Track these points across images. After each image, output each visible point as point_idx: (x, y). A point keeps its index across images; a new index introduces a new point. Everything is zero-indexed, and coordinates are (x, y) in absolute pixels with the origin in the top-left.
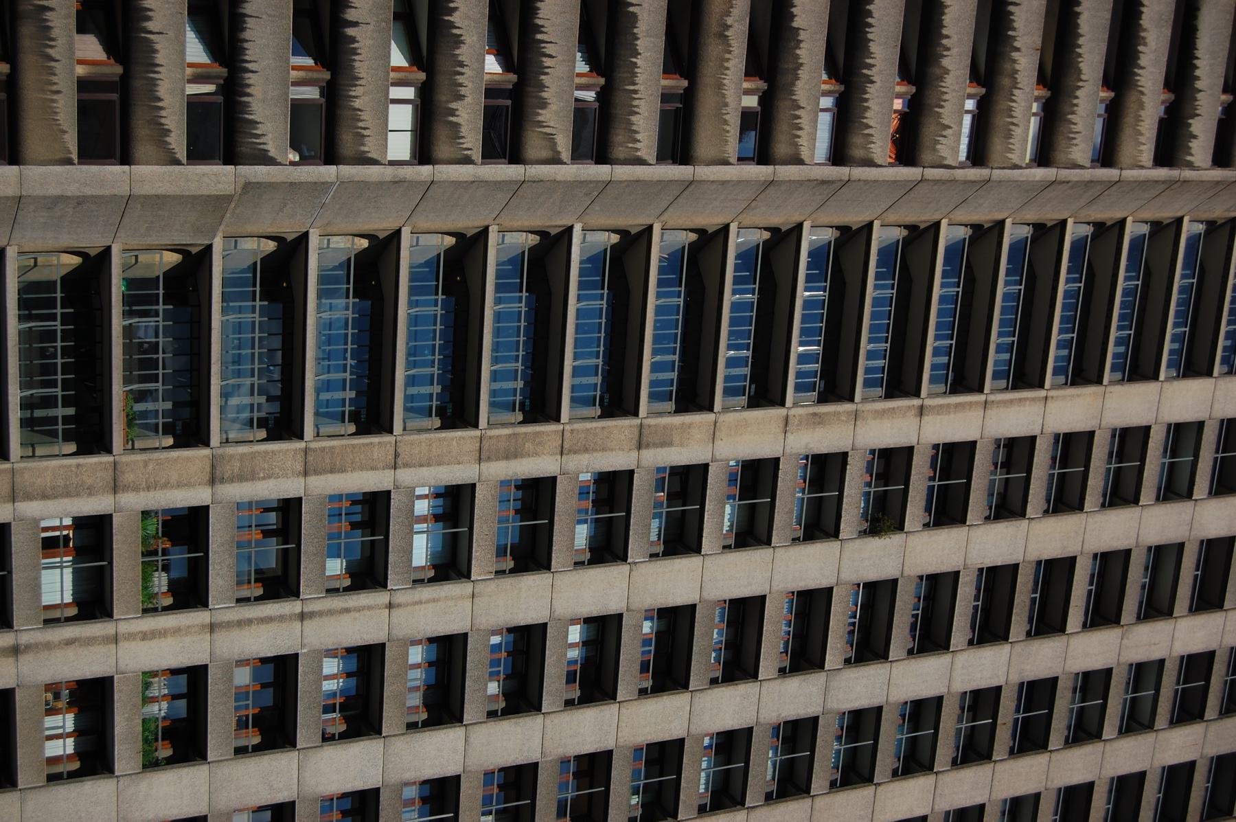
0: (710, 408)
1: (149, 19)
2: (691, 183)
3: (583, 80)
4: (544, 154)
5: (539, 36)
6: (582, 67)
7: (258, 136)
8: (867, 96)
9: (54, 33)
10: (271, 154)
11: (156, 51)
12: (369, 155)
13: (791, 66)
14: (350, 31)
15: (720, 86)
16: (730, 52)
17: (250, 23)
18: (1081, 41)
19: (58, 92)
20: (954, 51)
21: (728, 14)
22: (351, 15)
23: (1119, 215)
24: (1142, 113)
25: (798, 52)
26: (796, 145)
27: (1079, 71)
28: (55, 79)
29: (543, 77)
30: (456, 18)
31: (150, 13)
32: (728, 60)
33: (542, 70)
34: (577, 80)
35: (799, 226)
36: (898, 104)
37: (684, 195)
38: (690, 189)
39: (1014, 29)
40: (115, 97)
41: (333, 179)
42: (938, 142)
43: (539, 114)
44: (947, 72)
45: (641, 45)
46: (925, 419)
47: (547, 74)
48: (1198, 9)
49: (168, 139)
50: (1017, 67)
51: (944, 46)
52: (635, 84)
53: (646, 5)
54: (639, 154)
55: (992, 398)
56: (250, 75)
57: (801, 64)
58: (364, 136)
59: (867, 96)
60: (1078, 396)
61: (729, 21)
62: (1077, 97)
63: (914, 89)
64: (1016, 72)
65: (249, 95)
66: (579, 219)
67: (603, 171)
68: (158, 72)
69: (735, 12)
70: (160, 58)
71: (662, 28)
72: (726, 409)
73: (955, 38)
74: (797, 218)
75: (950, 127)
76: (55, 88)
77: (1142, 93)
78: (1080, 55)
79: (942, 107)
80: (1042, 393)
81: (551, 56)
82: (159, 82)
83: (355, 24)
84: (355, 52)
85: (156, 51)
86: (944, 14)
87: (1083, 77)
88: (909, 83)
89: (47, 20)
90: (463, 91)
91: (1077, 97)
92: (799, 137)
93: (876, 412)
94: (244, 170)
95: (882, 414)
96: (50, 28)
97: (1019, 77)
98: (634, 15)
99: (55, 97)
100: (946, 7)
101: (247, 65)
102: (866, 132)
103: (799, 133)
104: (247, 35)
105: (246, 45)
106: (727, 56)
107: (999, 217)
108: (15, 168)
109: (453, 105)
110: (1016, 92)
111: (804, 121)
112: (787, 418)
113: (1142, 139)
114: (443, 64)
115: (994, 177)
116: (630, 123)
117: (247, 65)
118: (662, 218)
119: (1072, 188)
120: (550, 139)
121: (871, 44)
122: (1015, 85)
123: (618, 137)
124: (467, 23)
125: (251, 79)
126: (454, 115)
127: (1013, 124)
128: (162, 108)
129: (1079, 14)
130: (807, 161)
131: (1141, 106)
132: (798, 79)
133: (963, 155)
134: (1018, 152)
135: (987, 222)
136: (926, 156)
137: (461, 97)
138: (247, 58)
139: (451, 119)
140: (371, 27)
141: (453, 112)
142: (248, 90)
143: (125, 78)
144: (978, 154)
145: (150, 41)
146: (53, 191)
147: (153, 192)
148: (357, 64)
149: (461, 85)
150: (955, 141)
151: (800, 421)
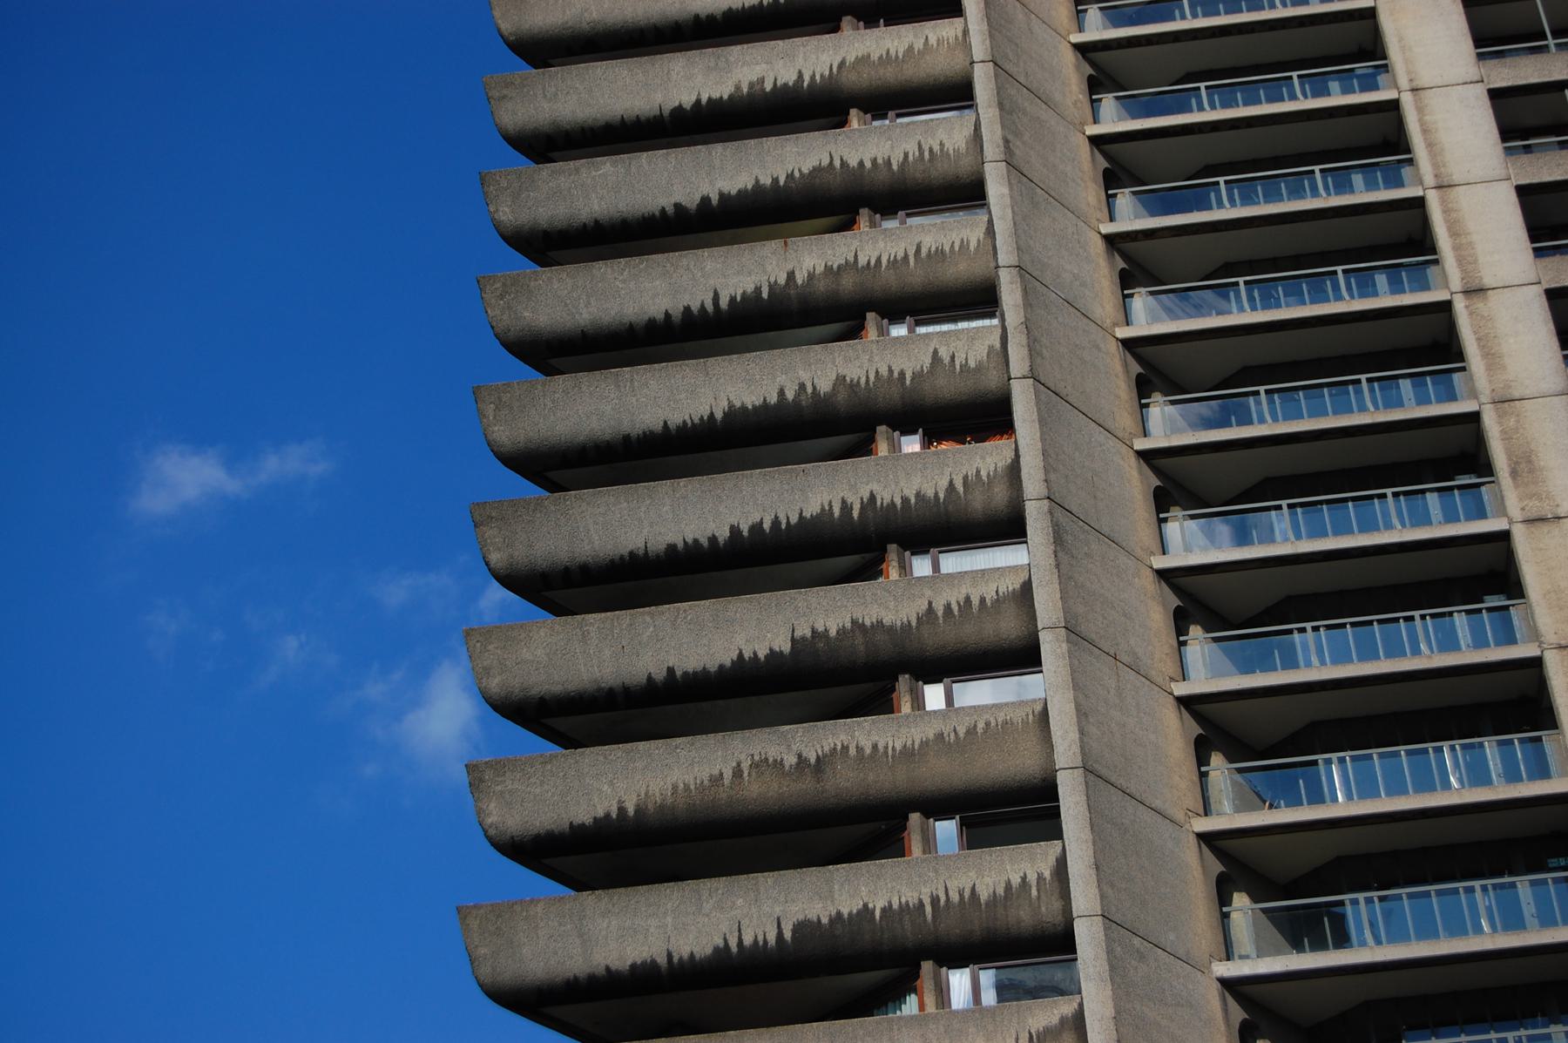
0: (1537, 663)
2: (1088, 770)
3: (930, 1000)
6: (911, 1005)
8: (898, 502)
13: (859, 640)
15: (908, 754)
16: (845, 748)
18: (766, 181)
20: (805, 376)
21: (778, 764)
23: (1069, 57)
24: (875, 57)
25: (833, 633)
26: (998, 601)
27: (817, 170)
32: (859, 749)
34: (931, 1008)
35: (1164, 575)
36: (912, 445)
37: (1121, 782)
38: (1104, 772)
39: (758, 290)
42: (964, 366)
44: (841, 379)
45: (848, 906)
46: (1488, 281)
48: (697, 17)
50: (820, 269)
51: (797, 395)
52: (921, 904)
53: (778, 910)
54: (1047, 874)
55: (1429, 180)
57: (854, 622)
59: (898, 502)
60: (1401, 40)
61: (790, 760)
62: (861, 163)
63: (882, 429)
64: (828, 269)
66: (1203, 969)
67: (1087, 935)
69: (773, 753)
71: (813, 874)
72: (1535, 635)
73: (781, 379)
74: (1149, 582)
75: (936, 352)
77: (842, 64)
78: (790, 176)
79: (902, 374)
80: (1407, 101)
86: (744, 408)
87: (826, 162)
88: (872, 440)
91: (861, 163)
92: (982, 600)
93: (1490, 368)
95: (1493, 359)
97: (836, 262)
98: (799, 928)
100: (731, 406)
102: (960, 488)
103: (975, 601)
106: (852, 751)
107: (1098, 246)
110: (862, 261)
111: (954, 596)
112: (1529, 521)
113: (919, 45)
115: (1013, 260)
116: (994, 900)
118: (1179, 816)
119: (1018, 134)
121: (807, 514)
122: (851, 266)
123: (1023, 917)
127: (918, 251)
129: (721, 195)
130: (1024, 577)
131: (864, 60)
132: (880, 623)
133: (995, 322)
134: (965, 233)
135: (1112, 263)
136: (992, 381)
144: (978, 299)
150: (963, 343)
151: (1531, 496)
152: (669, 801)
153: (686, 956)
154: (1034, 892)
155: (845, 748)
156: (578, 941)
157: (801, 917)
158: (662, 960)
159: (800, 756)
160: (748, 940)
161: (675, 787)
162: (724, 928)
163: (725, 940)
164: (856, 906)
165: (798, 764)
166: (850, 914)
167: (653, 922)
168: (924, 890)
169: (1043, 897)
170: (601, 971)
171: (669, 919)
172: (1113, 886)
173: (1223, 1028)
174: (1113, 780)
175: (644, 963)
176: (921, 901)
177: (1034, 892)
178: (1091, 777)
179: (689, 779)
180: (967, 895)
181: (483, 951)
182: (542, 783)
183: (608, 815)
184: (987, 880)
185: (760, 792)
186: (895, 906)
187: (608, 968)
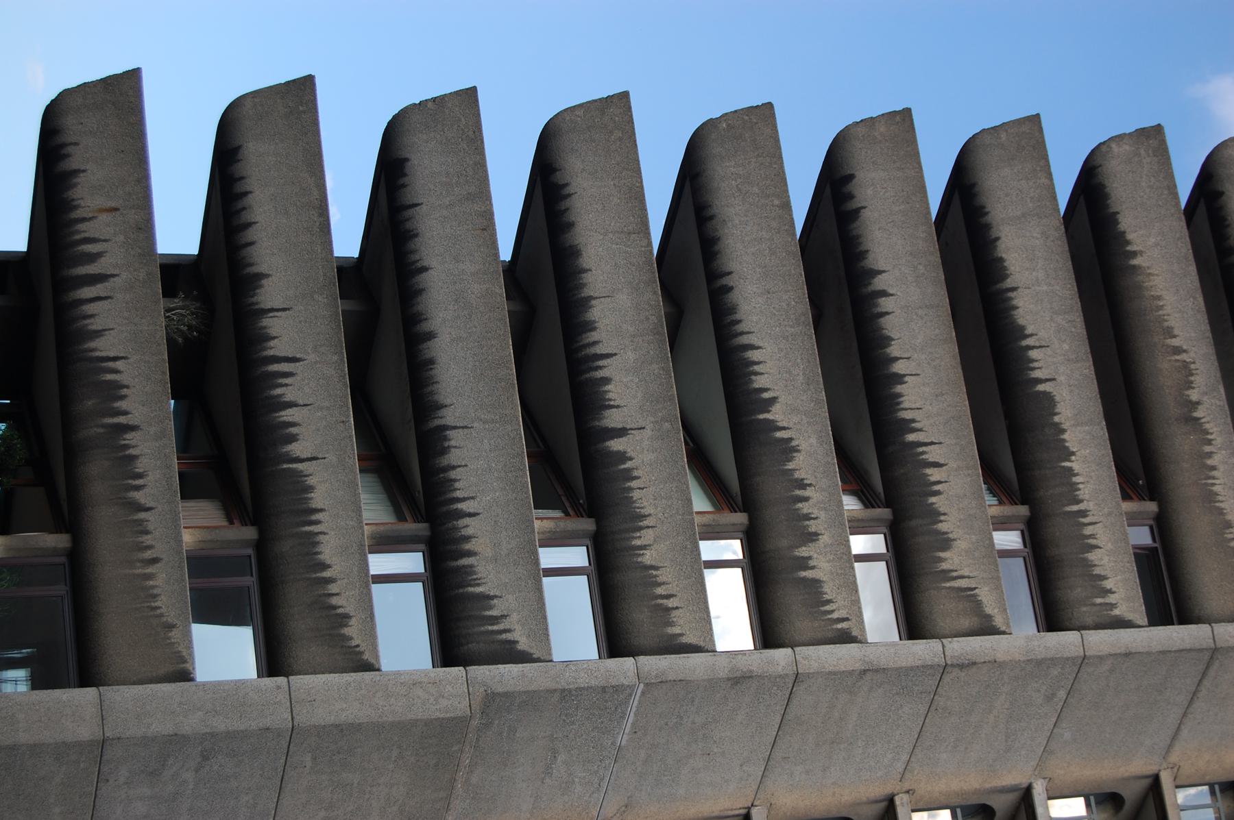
1: (293, 439)
4: (966, 623)
5: (911, 437)
7: (495, 620)
9: (140, 467)
10: (521, 647)
11: (310, 489)
12: (684, 640)
14: (616, 445)
15: (1210, 497)
16: (1209, 442)
17: (455, 438)
19: (155, 561)
21: (1189, 385)
22: (612, 419)
28: (147, 540)
29: (933, 500)
30: (776, 414)
31: (293, 430)
32: (1210, 455)
33: (929, 490)
37: (1203, 693)
38: (1212, 673)
40: (250, 581)
41: (631, 679)
43: (941, 560)
45: (1071, 438)
47: (937, 493)
49: (346, 631)
52: (1079, 502)
53: (1062, 378)
54: (1116, 612)
56: (466, 521)
58: (668, 610)
61: (1194, 395)
65: (470, 554)
68: (318, 522)
69: (1199, 380)
70: (318, 498)
76: (148, 554)
81: (937, 465)
82: (321, 538)
83: (622, 432)
84: (628, 476)
85: (310, 489)
89: (127, 447)
90: (813, 526)
94: (480, 672)
96: (133, 458)
98: (1048, 398)
99: (149, 570)
101: (460, 506)
104: (453, 457)
105: (453, 474)
106: (1207, 449)
108: (90, 693)
109: (803, 552)
114: (769, 488)
116: (1090, 565)
117: (460, 506)
118: (1173, 758)
120: (969, 597)
123: (1073, 591)
124: (795, 419)
125: (470, 527)
126: (807, 568)
128: (331, 580)
137: (813, 537)
138: (458, 494)
139: (803, 574)
140: (648, 433)
141: (804, 563)
142: (467, 546)
143: (261, 546)
145: (300, 474)
146: (160, 726)
147: (331, 719)
148: (636, 495)
149: (808, 517)
152: (1147, 293)
153: (1015, 302)
154: (1099, 601)
155: (1209, 442)
156: (1019, 213)
157: (1057, 398)
158: (1009, 283)
159: (1198, 403)
160: (1033, 354)
161: (1159, 298)
162: (1042, 334)
163: (1031, 335)
164: (1072, 445)
165: (1191, 402)
166: (1064, 440)
167: (1041, 275)
168: (1091, 504)
169: (1097, 608)
170: (994, 233)
171: (1045, 288)
172: (1111, 671)
173: (987, 786)
174: (1206, 683)
175: (1005, 269)
176: (1082, 501)
177: (1099, 601)
178: (1207, 656)
179: (1168, 310)
180: (1091, 541)
181: (1003, 136)
182: (1151, 187)
183: (1128, 243)
184: (1106, 559)
185: (1160, 374)
186: (1075, 479)
187: (998, 239)
